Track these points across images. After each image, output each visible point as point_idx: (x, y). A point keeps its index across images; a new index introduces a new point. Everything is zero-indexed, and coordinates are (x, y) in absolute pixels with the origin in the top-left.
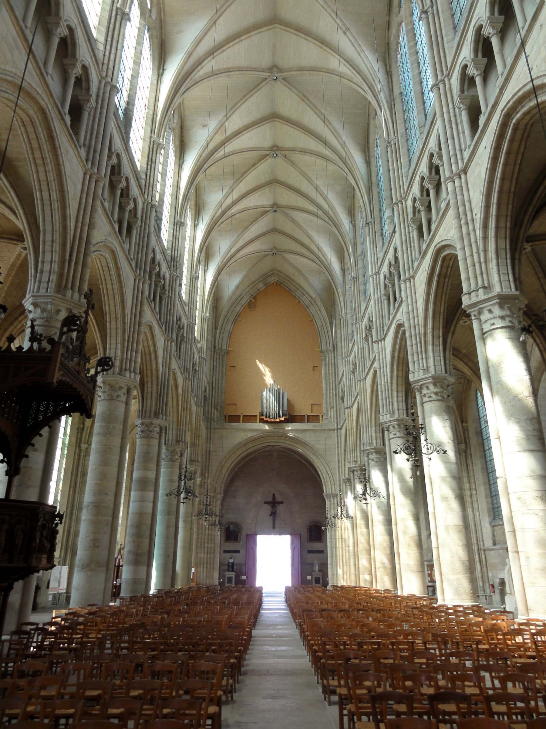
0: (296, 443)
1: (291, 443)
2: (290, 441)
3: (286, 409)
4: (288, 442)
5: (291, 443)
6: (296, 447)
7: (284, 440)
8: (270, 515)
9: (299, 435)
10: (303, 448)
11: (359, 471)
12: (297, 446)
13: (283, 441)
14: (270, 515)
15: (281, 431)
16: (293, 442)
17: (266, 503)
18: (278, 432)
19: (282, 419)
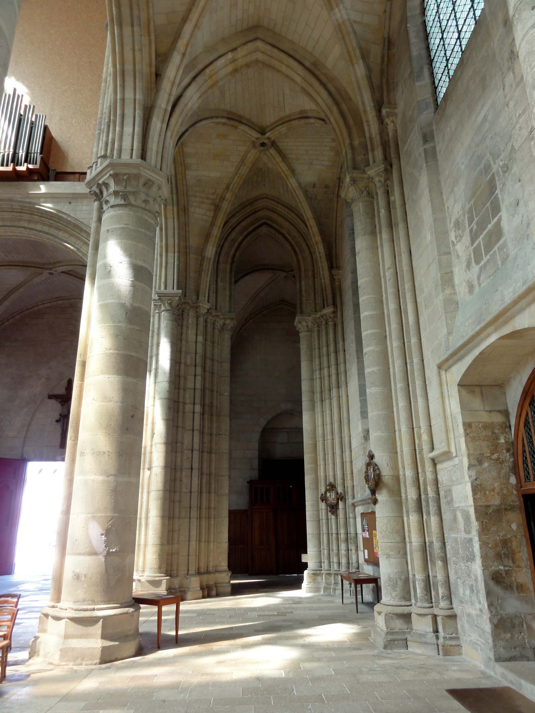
0: (57, 228)
1: (46, 229)
2: (44, 224)
3: (37, 146)
4: (39, 227)
5: (46, 229)
6: (56, 237)
7: (29, 221)
8: (57, 421)
9: (66, 208)
10: (73, 239)
11: (112, 183)
12: (61, 234)
13: (26, 225)
14: (57, 421)
15: (18, 197)
16: (50, 226)
17: (50, 397)
18: (10, 200)
19: (22, 168)
